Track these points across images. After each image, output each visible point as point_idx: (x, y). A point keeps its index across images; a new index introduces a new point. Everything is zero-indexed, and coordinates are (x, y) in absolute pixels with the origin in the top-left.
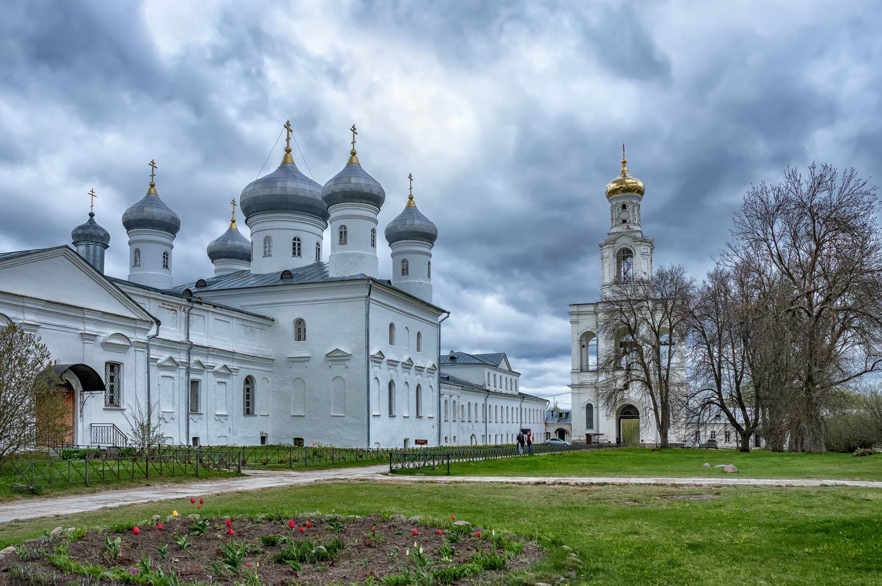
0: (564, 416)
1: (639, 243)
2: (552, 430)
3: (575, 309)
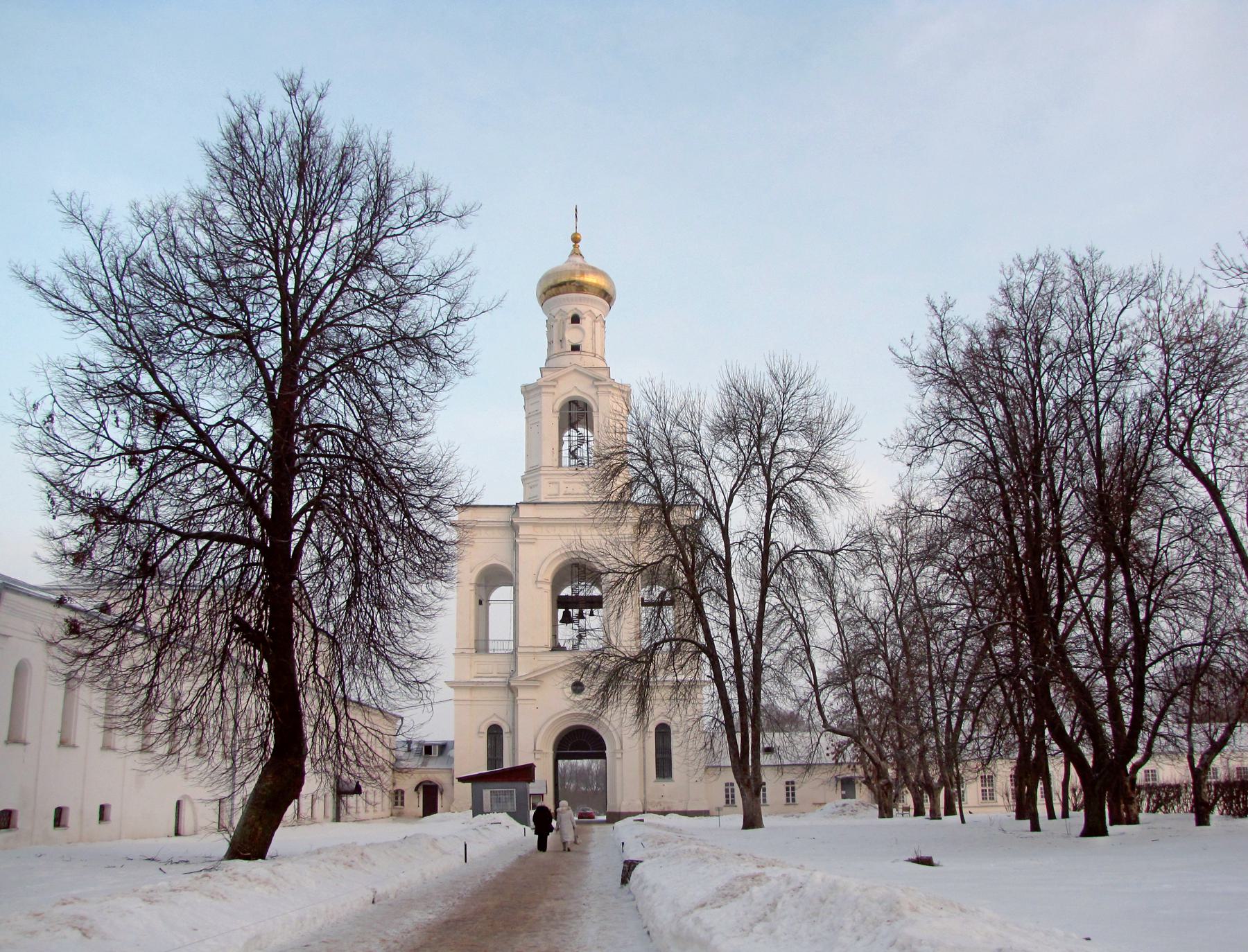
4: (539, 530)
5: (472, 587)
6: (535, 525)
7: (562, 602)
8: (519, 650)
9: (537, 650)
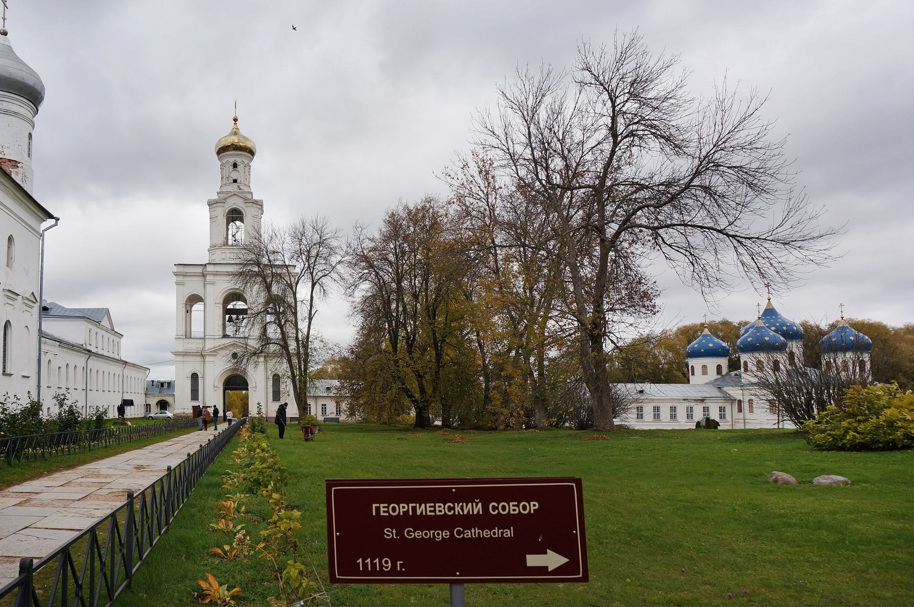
0: (165, 386)
1: (251, 204)
2: (153, 401)
3: (181, 269)
4: (218, 278)
5: (184, 305)
6: (214, 275)
7: (227, 311)
8: (207, 337)
9: (215, 337)
